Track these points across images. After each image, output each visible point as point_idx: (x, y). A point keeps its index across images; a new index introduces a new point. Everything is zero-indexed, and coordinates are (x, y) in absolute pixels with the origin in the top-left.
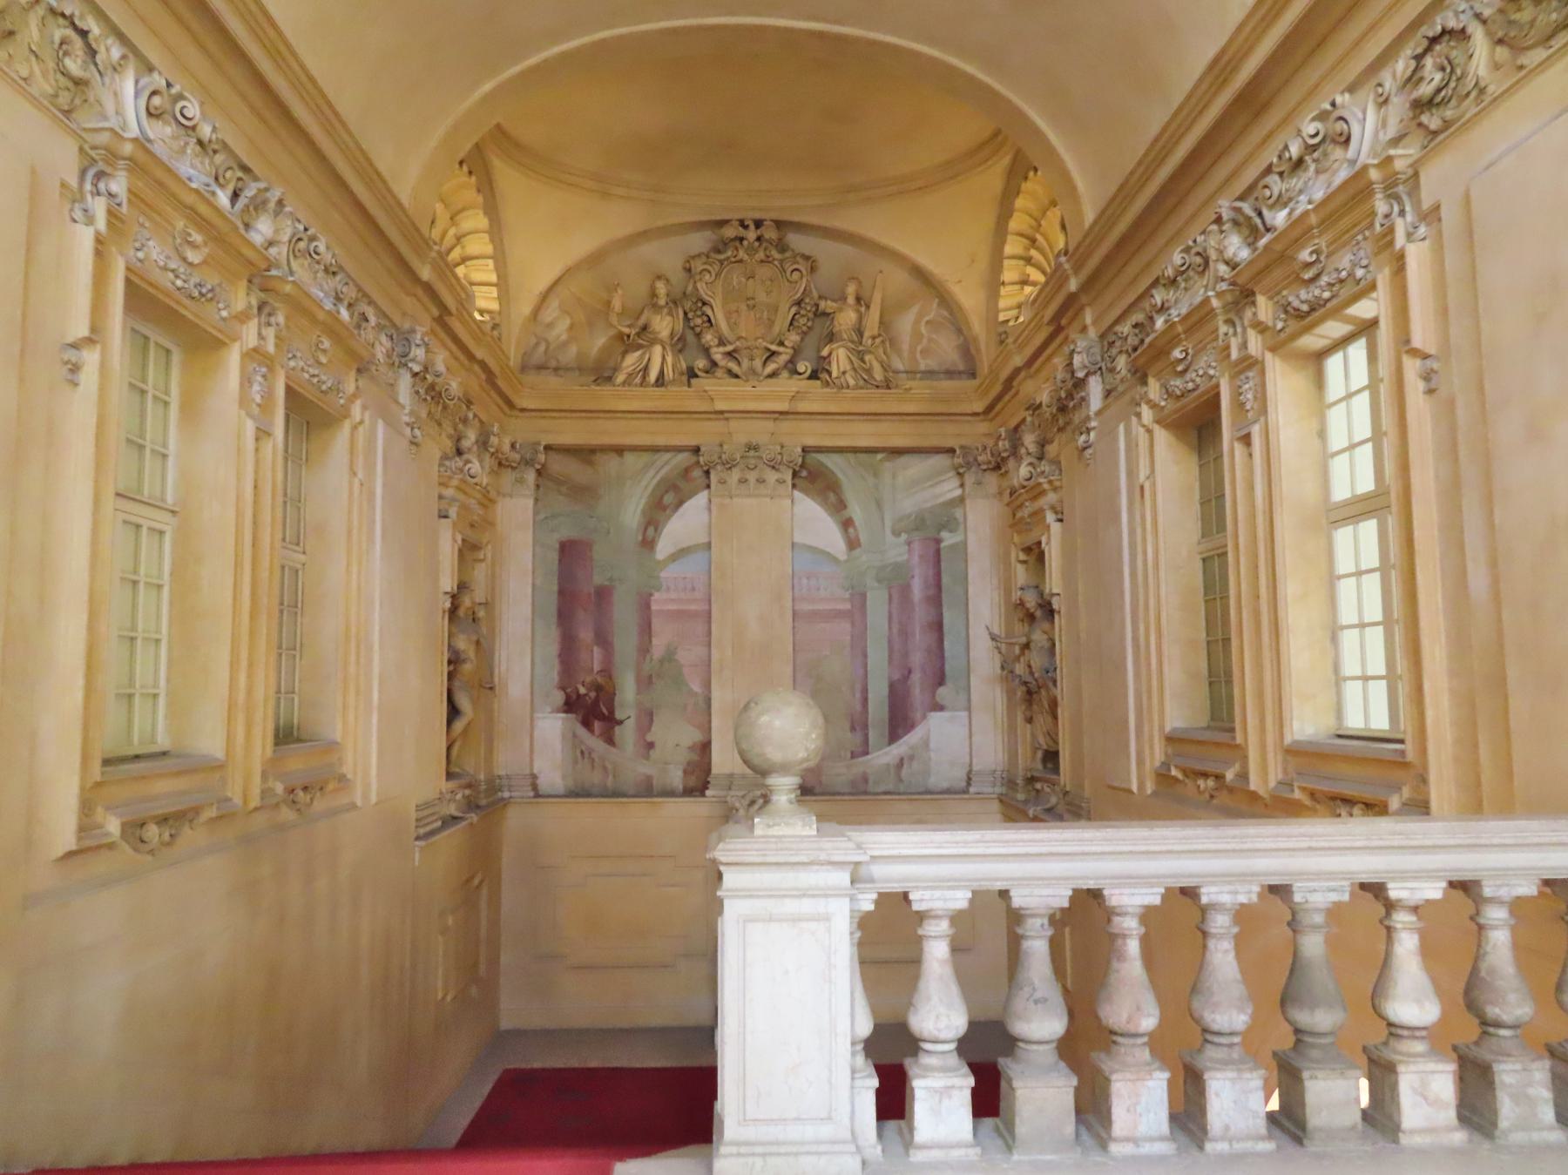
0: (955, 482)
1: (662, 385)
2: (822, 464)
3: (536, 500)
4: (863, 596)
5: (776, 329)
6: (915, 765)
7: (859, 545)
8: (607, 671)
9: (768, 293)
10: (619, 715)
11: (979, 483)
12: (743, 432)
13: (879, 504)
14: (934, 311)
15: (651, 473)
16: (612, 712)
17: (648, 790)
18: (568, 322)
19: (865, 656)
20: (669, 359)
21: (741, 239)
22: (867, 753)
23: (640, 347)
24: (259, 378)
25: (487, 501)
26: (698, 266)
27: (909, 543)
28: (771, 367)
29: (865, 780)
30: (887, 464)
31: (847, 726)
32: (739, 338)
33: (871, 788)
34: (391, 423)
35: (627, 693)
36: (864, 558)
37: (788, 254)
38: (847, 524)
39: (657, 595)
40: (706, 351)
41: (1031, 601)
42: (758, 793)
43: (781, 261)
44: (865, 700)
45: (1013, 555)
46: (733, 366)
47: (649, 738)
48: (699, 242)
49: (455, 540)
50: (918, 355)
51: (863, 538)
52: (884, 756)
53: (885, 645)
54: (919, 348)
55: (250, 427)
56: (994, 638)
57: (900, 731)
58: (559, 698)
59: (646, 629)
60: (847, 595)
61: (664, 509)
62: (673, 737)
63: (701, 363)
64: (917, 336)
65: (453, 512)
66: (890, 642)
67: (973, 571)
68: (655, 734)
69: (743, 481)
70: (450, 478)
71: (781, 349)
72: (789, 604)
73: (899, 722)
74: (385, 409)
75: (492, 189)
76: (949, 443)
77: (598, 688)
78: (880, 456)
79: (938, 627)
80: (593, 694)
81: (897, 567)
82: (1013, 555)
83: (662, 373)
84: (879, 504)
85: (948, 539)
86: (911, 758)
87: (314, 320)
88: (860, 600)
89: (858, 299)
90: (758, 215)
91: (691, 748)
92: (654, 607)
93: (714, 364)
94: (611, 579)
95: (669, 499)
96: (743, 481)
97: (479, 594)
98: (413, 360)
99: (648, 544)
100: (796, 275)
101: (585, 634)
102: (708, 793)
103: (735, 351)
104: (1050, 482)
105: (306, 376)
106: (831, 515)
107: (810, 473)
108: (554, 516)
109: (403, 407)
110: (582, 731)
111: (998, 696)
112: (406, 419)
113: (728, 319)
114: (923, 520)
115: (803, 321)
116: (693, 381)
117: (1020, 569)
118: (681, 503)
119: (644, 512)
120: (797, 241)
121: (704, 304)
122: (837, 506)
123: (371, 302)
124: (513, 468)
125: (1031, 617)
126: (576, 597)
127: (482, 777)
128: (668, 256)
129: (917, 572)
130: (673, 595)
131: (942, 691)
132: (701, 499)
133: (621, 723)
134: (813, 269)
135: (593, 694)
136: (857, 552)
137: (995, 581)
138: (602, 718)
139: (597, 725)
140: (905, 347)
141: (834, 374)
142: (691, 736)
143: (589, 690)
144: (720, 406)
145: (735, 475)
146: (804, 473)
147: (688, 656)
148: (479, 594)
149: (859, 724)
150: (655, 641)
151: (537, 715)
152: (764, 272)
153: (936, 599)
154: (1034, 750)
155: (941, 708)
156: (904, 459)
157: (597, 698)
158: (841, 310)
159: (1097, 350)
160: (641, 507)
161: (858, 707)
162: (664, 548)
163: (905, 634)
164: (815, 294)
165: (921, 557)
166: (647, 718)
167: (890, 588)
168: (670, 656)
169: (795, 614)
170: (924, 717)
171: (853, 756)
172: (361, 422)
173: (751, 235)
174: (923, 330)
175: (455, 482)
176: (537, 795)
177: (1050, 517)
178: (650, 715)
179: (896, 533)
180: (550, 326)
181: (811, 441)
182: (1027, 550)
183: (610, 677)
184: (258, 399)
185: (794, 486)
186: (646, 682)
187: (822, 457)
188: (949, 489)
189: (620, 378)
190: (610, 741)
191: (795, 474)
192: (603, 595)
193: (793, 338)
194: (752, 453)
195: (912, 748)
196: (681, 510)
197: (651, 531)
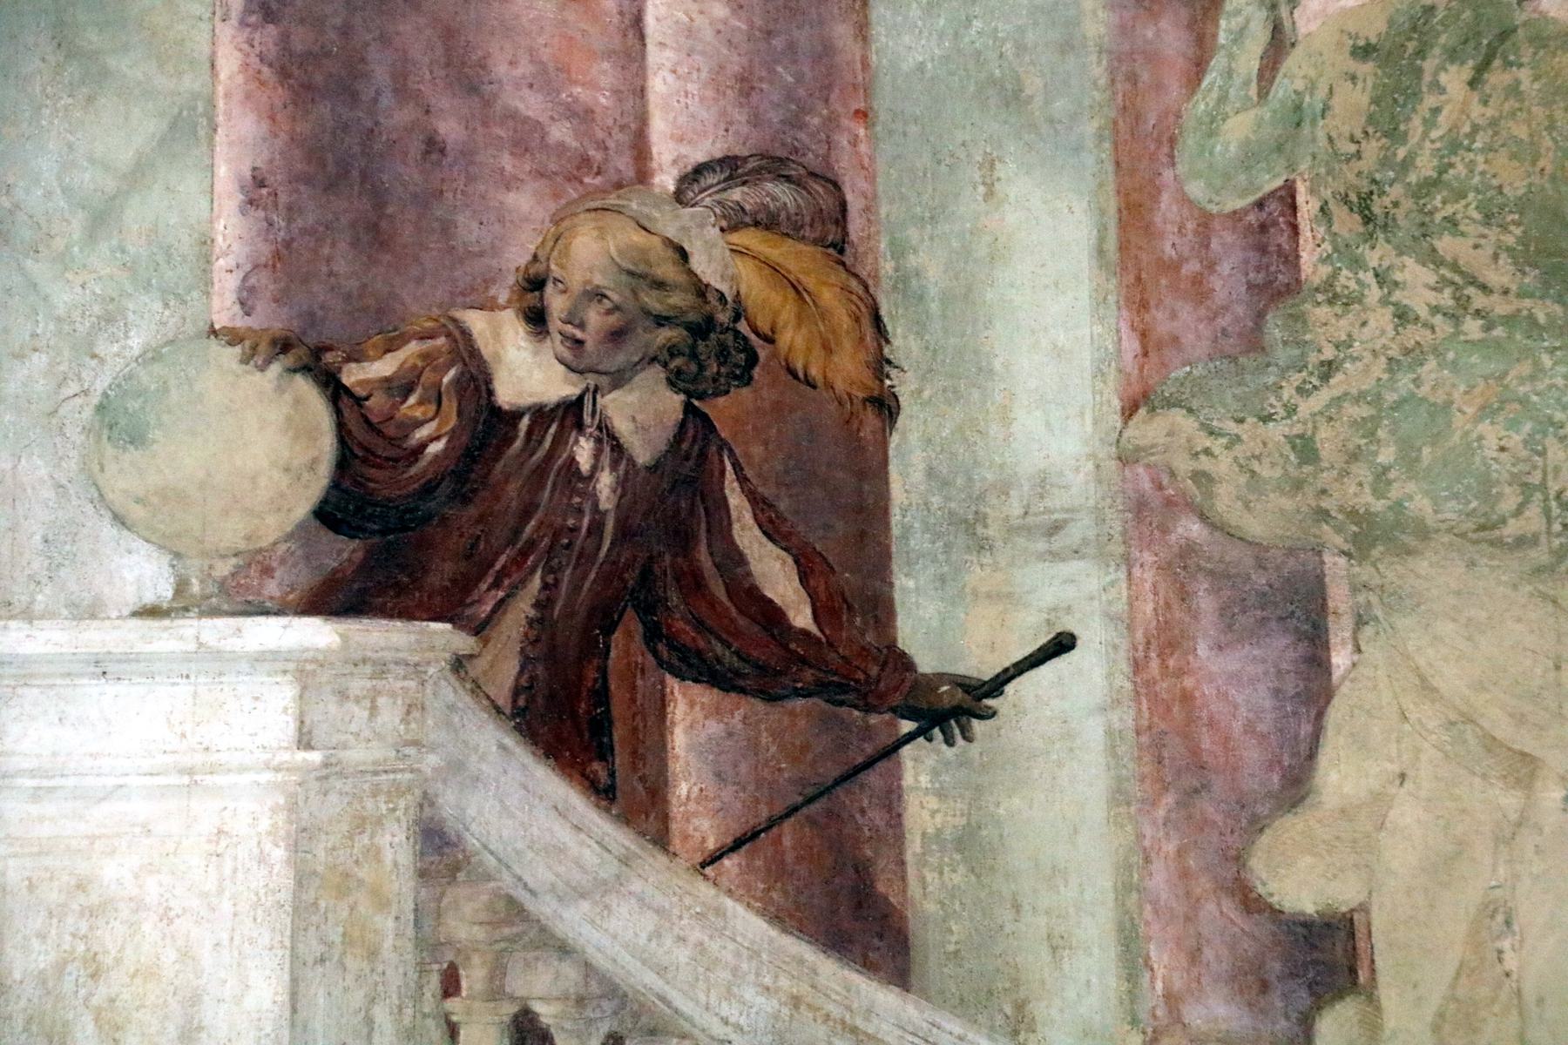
8: (796, 184)
10: (937, 625)
47: (1299, 882)
58: (262, 448)
77: (709, 346)
110: (524, 811)
133: (956, 707)
135: (642, 412)
138: (752, 659)
157: (695, 437)
178: (1295, 614)
183: (831, 230)
190: (854, 911)
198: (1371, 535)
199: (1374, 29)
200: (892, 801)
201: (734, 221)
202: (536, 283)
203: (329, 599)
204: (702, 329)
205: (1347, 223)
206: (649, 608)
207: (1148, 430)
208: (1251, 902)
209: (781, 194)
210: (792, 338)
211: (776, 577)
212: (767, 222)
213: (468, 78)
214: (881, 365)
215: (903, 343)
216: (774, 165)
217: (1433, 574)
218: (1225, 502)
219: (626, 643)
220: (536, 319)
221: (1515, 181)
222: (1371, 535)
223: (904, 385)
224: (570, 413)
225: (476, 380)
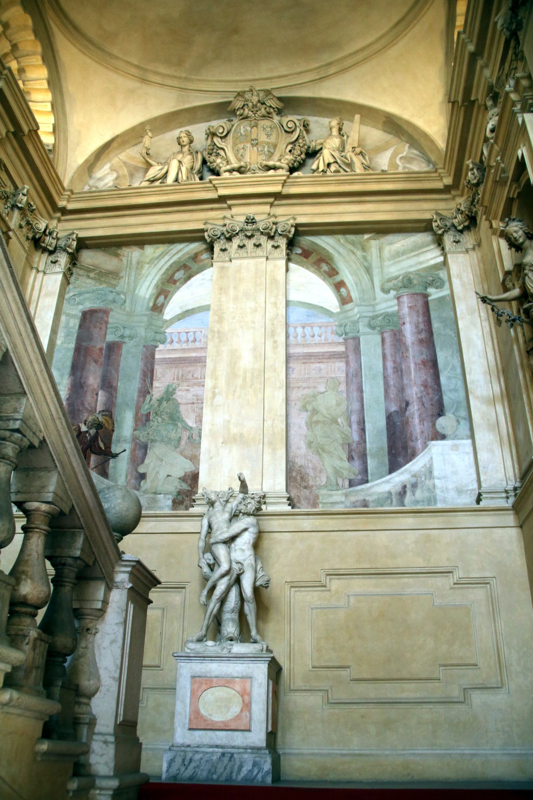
2: (313, 242)
4: (357, 340)
6: (419, 494)
7: (351, 301)
8: (108, 412)
9: (268, 136)
10: (114, 449)
11: (457, 242)
13: (368, 270)
14: (406, 150)
15: (167, 258)
16: (108, 446)
18: (115, 175)
19: (360, 390)
22: (367, 482)
27: (398, 298)
30: (373, 243)
31: (345, 456)
35: (126, 426)
36: (356, 310)
38: (339, 286)
39: (161, 347)
44: (363, 430)
47: (141, 470)
51: (354, 295)
53: (382, 382)
56: (484, 300)
57: (401, 460)
59: (148, 374)
60: (341, 340)
61: (175, 282)
64: (392, 163)
66: (385, 378)
67: (461, 308)
68: (149, 465)
69: (241, 247)
72: (282, 339)
73: (399, 451)
75: (54, 57)
76: (427, 216)
77: (99, 426)
78: (366, 236)
79: (433, 364)
81: (388, 317)
84: (368, 270)
85: (434, 294)
86: (414, 486)
88: (354, 344)
91: (183, 479)
92: (157, 356)
94: (122, 336)
99: (158, 308)
101: (93, 379)
107: (304, 251)
108: (80, 294)
111: (501, 411)
113: (236, 156)
114: (410, 281)
118: (189, 277)
119: (157, 286)
129: (407, 320)
130: (176, 346)
131: (441, 422)
132: (208, 273)
133: (115, 456)
135: (93, 432)
136: (349, 306)
138: (99, 452)
139: (93, 459)
142: (180, 466)
143: (90, 428)
145: (236, 242)
149: (357, 453)
150: (156, 384)
152: (266, 123)
153: (428, 340)
155: (443, 437)
156: (390, 238)
157: (97, 433)
160: (155, 282)
161: (356, 437)
162: (171, 310)
163: (399, 370)
165: (410, 308)
166: (142, 449)
167: (382, 334)
168: (169, 395)
169: (288, 358)
170: (425, 446)
174: (398, 161)
178: (145, 448)
180: (100, 179)
181: (301, 220)
183: (111, 416)
186: (143, 420)
188: (432, 257)
192: (113, 349)
194: (249, 227)
195: (414, 476)
196: (189, 283)
197: (162, 298)
198: (152, 441)
199: (159, 398)
200: (109, 464)
201: (103, 415)
202: (86, 421)
204: (99, 424)
205: (154, 415)
206: (91, 448)
207: (135, 432)
208: (137, 472)
209: (107, 413)
210: (106, 425)
211: (102, 445)
212: (106, 415)
213: (83, 404)
214: (113, 427)
215: (116, 425)
216: (107, 411)
217: (157, 444)
218: (141, 439)
219: (88, 451)
220: (85, 424)
221: (169, 411)
222: (152, 441)
223: (115, 429)
224: (87, 432)
225: (79, 428)
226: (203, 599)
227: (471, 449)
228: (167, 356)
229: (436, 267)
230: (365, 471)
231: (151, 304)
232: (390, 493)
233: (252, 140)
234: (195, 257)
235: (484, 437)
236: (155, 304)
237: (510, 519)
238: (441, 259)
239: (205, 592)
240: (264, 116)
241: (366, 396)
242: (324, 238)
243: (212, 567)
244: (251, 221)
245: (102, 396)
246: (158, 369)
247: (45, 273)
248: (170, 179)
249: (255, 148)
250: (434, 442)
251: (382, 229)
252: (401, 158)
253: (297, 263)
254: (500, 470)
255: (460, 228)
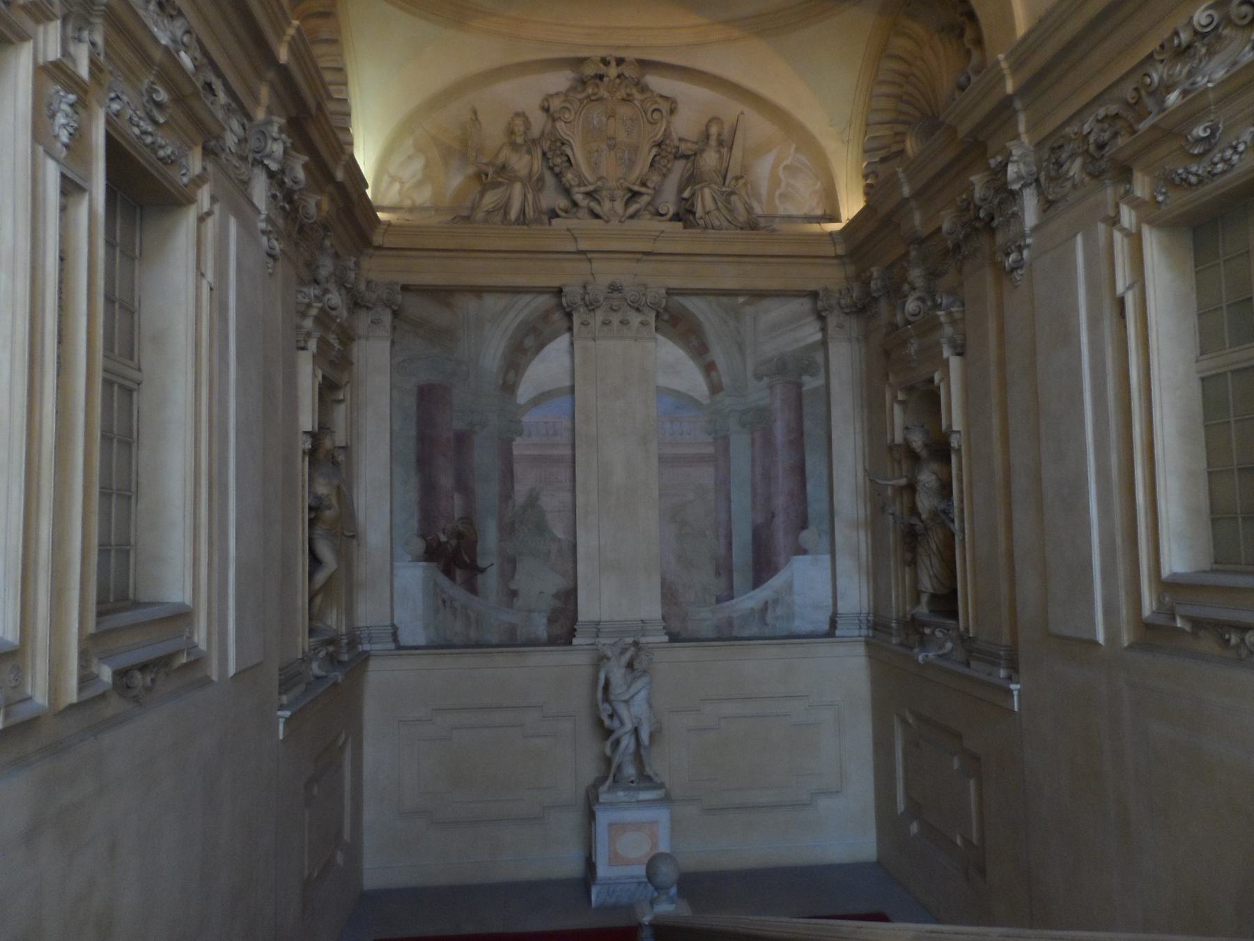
0: (816, 325)
1: (524, 223)
2: (683, 306)
3: (393, 343)
4: (726, 439)
5: (636, 173)
8: (468, 519)
9: (629, 133)
10: (482, 563)
11: (840, 326)
12: (606, 273)
13: (741, 347)
16: (474, 561)
17: (513, 641)
19: (729, 499)
20: (530, 197)
21: (601, 77)
22: (732, 598)
23: (500, 184)
24: (65, 107)
25: (347, 337)
26: (556, 104)
27: (771, 387)
28: (633, 208)
29: (730, 623)
32: (600, 178)
33: (735, 633)
34: (246, 226)
35: (490, 538)
37: (648, 95)
38: (709, 368)
39: (518, 440)
40: (567, 192)
41: (917, 441)
42: (630, 640)
43: (642, 101)
44: (730, 544)
45: (888, 396)
46: (593, 205)
47: (513, 586)
48: (560, 81)
49: (315, 375)
50: (777, 201)
51: (725, 380)
52: (749, 601)
54: (777, 193)
55: (52, 173)
58: (419, 545)
59: (508, 476)
60: (710, 439)
62: (538, 584)
63: (562, 203)
65: (313, 345)
69: (606, 323)
70: (309, 305)
71: (643, 190)
73: (764, 566)
74: (236, 197)
76: (812, 286)
77: (460, 536)
78: (741, 300)
79: (800, 471)
80: (454, 542)
82: (888, 396)
83: (523, 211)
84: (741, 347)
85: (811, 383)
87: (146, 59)
88: (723, 443)
89: (721, 143)
90: (620, 54)
91: (556, 596)
92: (515, 452)
93: (575, 204)
95: (529, 342)
96: (606, 323)
97: (340, 438)
98: (269, 156)
99: (509, 388)
100: (656, 115)
101: (446, 480)
102: (575, 641)
103: (595, 191)
104: (950, 314)
105: (136, 131)
106: (693, 358)
109: (259, 212)
110: (443, 581)
111: (863, 539)
112: (263, 225)
115: (664, 162)
116: (554, 221)
117: (897, 409)
120: (656, 82)
121: (563, 144)
122: (700, 351)
123: (220, 75)
124: (368, 308)
125: (914, 457)
126: (436, 443)
127: (344, 630)
128: (526, 95)
132: (564, 340)
133: (482, 571)
134: (672, 112)
135: (454, 542)
137: (858, 425)
139: (459, 574)
140: (764, 190)
141: (698, 215)
142: (553, 583)
144: (583, 245)
145: (599, 316)
146: (666, 317)
147: (552, 502)
148: (340, 438)
149: (724, 568)
150: (517, 487)
151: (396, 564)
152: (625, 111)
153: (798, 441)
154: (917, 595)
156: (766, 303)
158: (702, 151)
159: (1031, 159)
162: (525, 392)
164: (674, 136)
166: (510, 564)
170: (788, 560)
171: (718, 601)
172: (209, 214)
173: (613, 71)
175: (314, 312)
176: (399, 648)
177: (947, 352)
179: (759, 377)
181: (674, 283)
182: (910, 389)
184: (64, 137)
185: (657, 329)
186: (508, 530)
187: (681, 300)
188: (810, 333)
189: (480, 215)
190: (472, 588)
191: (657, 316)
192: (462, 440)
193: (655, 178)
194: (616, 295)
197: (511, 375)
203: (426, 560)
211: (466, 559)
224: (447, 543)
226: (608, 751)
227: (828, 564)
228: (527, 452)
229: (812, 347)
230: (731, 586)
231: (501, 382)
232: (752, 609)
233: (609, 139)
234: (545, 317)
235: (845, 563)
236: (505, 382)
237: (861, 649)
238: (819, 336)
239: (609, 743)
240: (623, 100)
241: (733, 506)
242: (694, 299)
243: (611, 716)
244: (614, 288)
245: (458, 501)
246: (518, 468)
247: (367, 338)
248: (513, 214)
249: (613, 153)
250: (796, 557)
251: (758, 295)
252: (785, 167)
253: (664, 335)
254: (855, 596)
255: (847, 311)
